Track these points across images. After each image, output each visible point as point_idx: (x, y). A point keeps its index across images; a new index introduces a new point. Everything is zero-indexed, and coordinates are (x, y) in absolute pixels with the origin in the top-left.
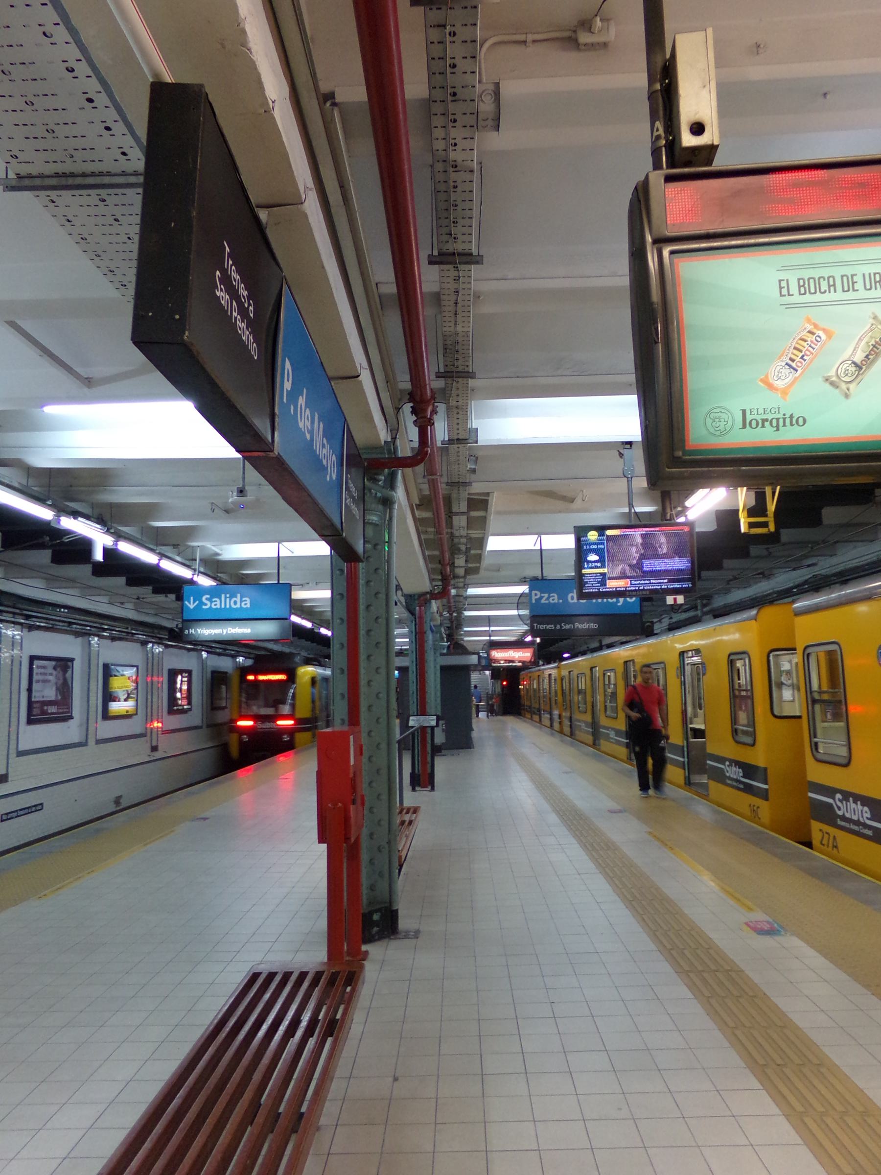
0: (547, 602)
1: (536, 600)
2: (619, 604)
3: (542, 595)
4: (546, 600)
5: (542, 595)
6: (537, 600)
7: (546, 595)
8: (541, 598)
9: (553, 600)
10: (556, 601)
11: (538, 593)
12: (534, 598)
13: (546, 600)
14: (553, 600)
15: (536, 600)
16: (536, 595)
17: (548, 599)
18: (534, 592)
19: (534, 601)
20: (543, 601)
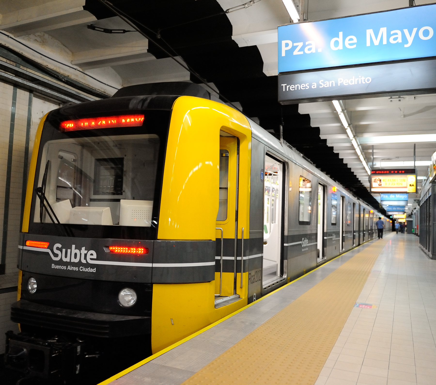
0: (302, 53)
1: (286, 51)
2: (406, 46)
3: (295, 44)
4: (300, 51)
5: (295, 44)
6: (289, 52)
7: (300, 44)
8: (294, 48)
9: (309, 49)
10: (313, 51)
11: (290, 42)
12: (284, 49)
13: (300, 51)
14: (309, 49)
15: (286, 51)
16: (287, 45)
17: (302, 49)
18: (284, 42)
19: (283, 54)
20: (296, 53)
